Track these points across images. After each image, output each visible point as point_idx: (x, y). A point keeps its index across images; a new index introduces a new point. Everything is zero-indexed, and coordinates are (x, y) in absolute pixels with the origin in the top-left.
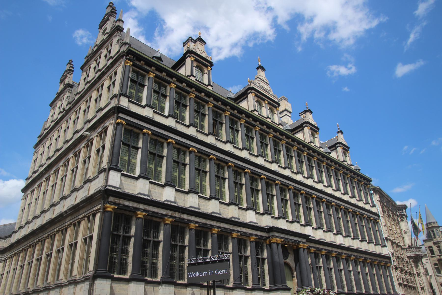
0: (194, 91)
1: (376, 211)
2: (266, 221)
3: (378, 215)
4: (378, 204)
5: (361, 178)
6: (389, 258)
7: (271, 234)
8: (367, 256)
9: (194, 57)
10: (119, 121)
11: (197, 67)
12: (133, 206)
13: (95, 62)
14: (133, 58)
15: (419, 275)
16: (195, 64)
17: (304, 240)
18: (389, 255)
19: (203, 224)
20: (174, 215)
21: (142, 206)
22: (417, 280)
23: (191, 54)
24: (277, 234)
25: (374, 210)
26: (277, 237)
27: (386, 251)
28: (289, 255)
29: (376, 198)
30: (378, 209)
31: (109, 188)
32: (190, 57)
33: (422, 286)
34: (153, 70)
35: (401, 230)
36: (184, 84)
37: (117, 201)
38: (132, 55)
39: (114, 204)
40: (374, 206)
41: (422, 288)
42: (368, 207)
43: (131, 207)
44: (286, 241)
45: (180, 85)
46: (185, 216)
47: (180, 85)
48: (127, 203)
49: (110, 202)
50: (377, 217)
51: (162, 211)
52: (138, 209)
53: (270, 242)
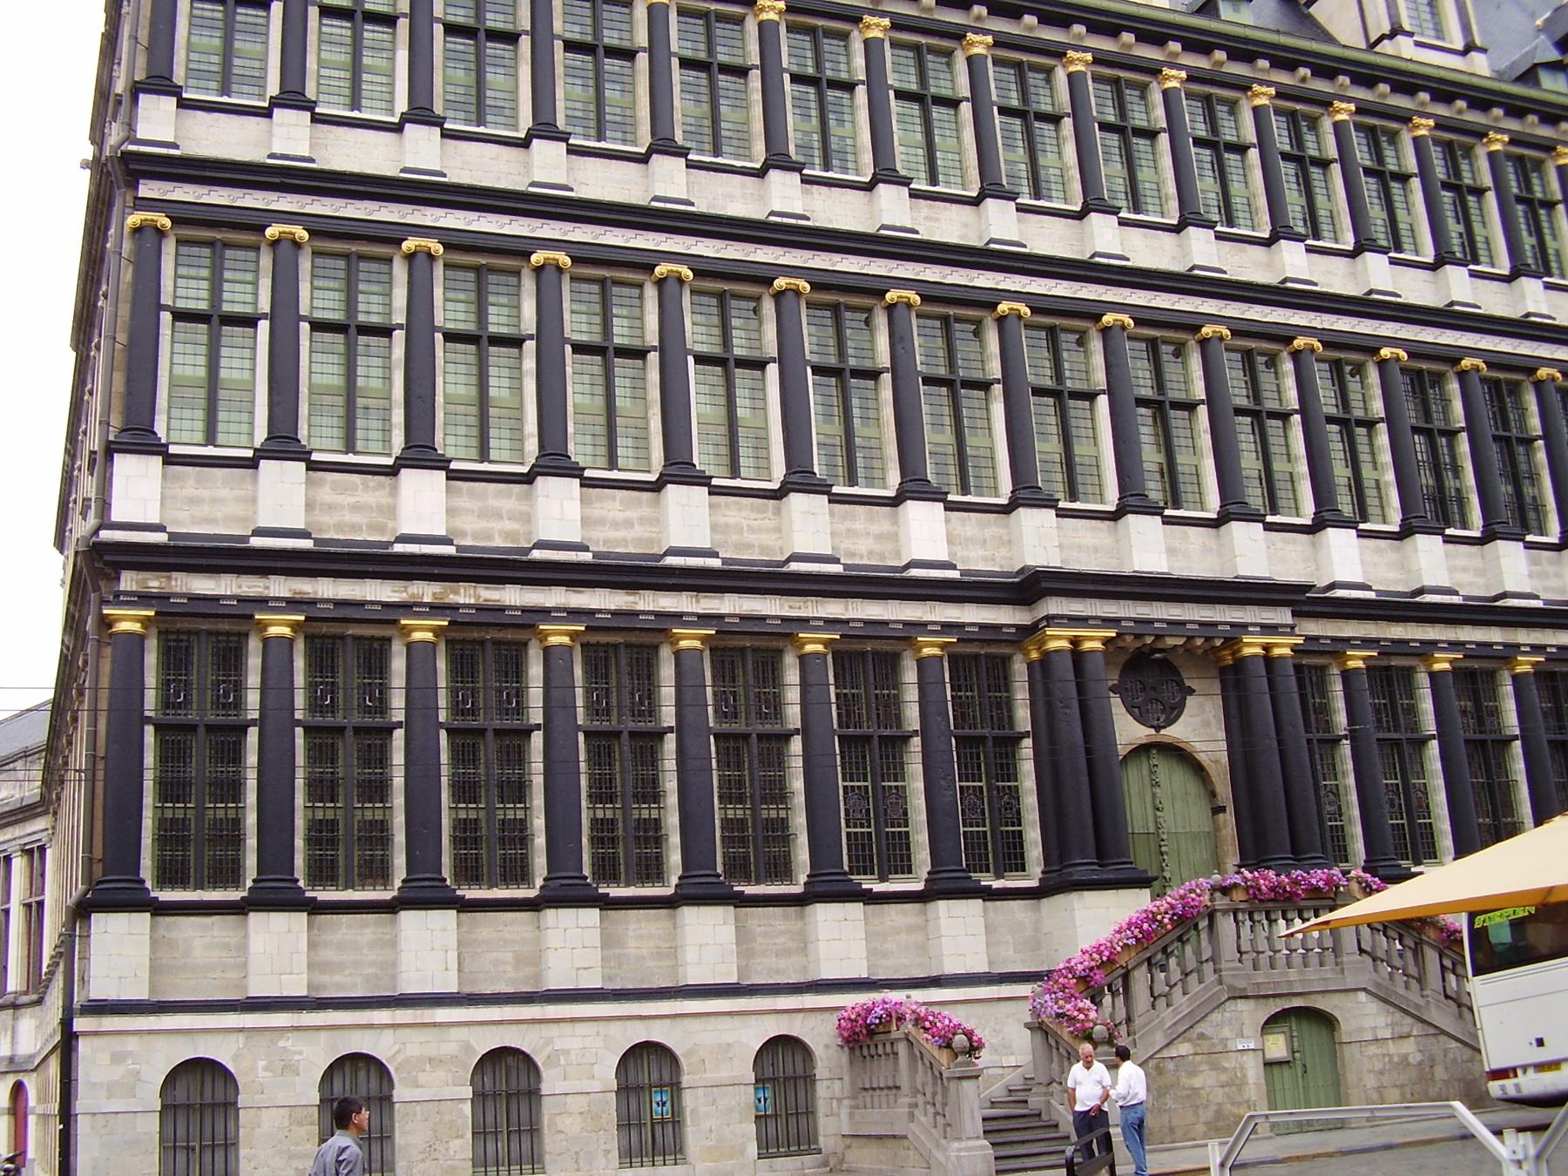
12: (236, 591)
17: (1283, 616)
19: (616, 613)
20: (453, 598)
21: (280, 587)
26: (1081, 621)
28: (1191, 701)
31: (105, 535)
37: (155, 584)
44: (1138, 636)
46: (513, 596)
48: (203, 585)
49: (126, 593)
52: (262, 602)
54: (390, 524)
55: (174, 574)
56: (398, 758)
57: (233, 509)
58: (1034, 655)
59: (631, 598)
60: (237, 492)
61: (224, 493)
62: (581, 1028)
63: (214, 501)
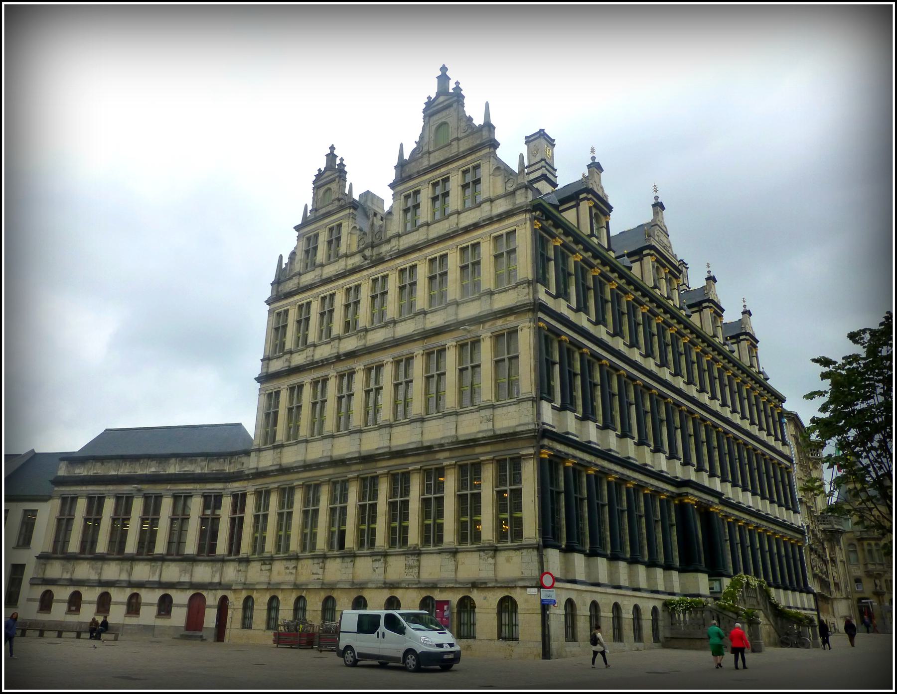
2: (678, 470)
3: (791, 461)
6: (802, 533)
7: (685, 490)
8: (777, 528)
15: (833, 561)
16: (594, 211)
17: (717, 501)
18: (803, 526)
22: (830, 572)
24: (691, 491)
25: (786, 450)
26: (692, 495)
27: (799, 520)
29: (789, 430)
30: (791, 450)
33: (837, 581)
38: (541, 210)
40: (785, 443)
41: (837, 585)
42: (779, 446)
46: (606, 464)
50: (789, 464)
53: (680, 501)
62: (627, 598)
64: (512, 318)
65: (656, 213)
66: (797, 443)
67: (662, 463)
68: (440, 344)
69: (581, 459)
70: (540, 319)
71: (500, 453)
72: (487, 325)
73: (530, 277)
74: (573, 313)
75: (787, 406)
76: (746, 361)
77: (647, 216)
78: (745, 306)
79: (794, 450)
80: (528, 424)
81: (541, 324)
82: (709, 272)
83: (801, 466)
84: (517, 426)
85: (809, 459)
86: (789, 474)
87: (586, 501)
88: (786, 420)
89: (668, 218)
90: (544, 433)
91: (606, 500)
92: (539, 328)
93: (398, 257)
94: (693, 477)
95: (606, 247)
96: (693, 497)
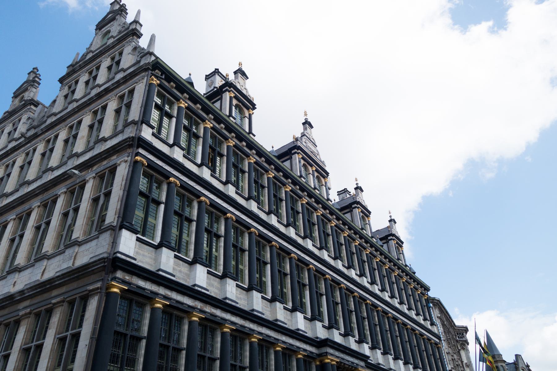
0: (233, 137)
1: (436, 332)
3: (439, 338)
4: (438, 322)
5: (418, 284)
9: (234, 93)
10: (138, 158)
11: (237, 106)
12: (150, 288)
13: (87, 75)
14: (161, 75)
16: (235, 102)
17: (362, 364)
19: (241, 326)
21: (162, 291)
23: (230, 88)
25: (434, 329)
26: (332, 355)
29: (435, 313)
30: (438, 329)
31: (119, 255)
32: (229, 92)
34: (185, 98)
35: (462, 362)
36: (222, 125)
37: (127, 278)
39: (124, 282)
42: (428, 324)
43: (147, 289)
45: (217, 126)
46: (218, 313)
47: (217, 126)
48: (142, 283)
49: (119, 279)
50: (437, 340)
51: (189, 301)
52: (157, 294)
53: (321, 361)
54: (188, 280)
55: (134, 277)
56: (183, 361)
57: (148, 260)
58: (318, 363)
59: (244, 322)
60: (150, 255)
61: (146, 254)
63: (143, 255)
64: (115, 157)
65: (305, 129)
66: (443, 325)
67: (300, 322)
68: (54, 193)
69: (178, 302)
70: (138, 154)
71: (70, 294)
72: (95, 168)
73: (137, 119)
74: (195, 167)
75: (431, 294)
76: (394, 255)
77: (298, 131)
78: (390, 216)
79: (441, 330)
80: (101, 254)
81: (138, 158)
82: (357, 184)
83: (449, 343)
84: (91, 258)
85: (457, 341)
86: (438, 348)
87: (184, 352)
88: (431, 305)
89: (314, 133)
90: (116, 263)
91: (218, 354)
92: (136, 162)
93: (46, 131)
94: (338, 339)
95: (247, 130)
96: (333, 357)
